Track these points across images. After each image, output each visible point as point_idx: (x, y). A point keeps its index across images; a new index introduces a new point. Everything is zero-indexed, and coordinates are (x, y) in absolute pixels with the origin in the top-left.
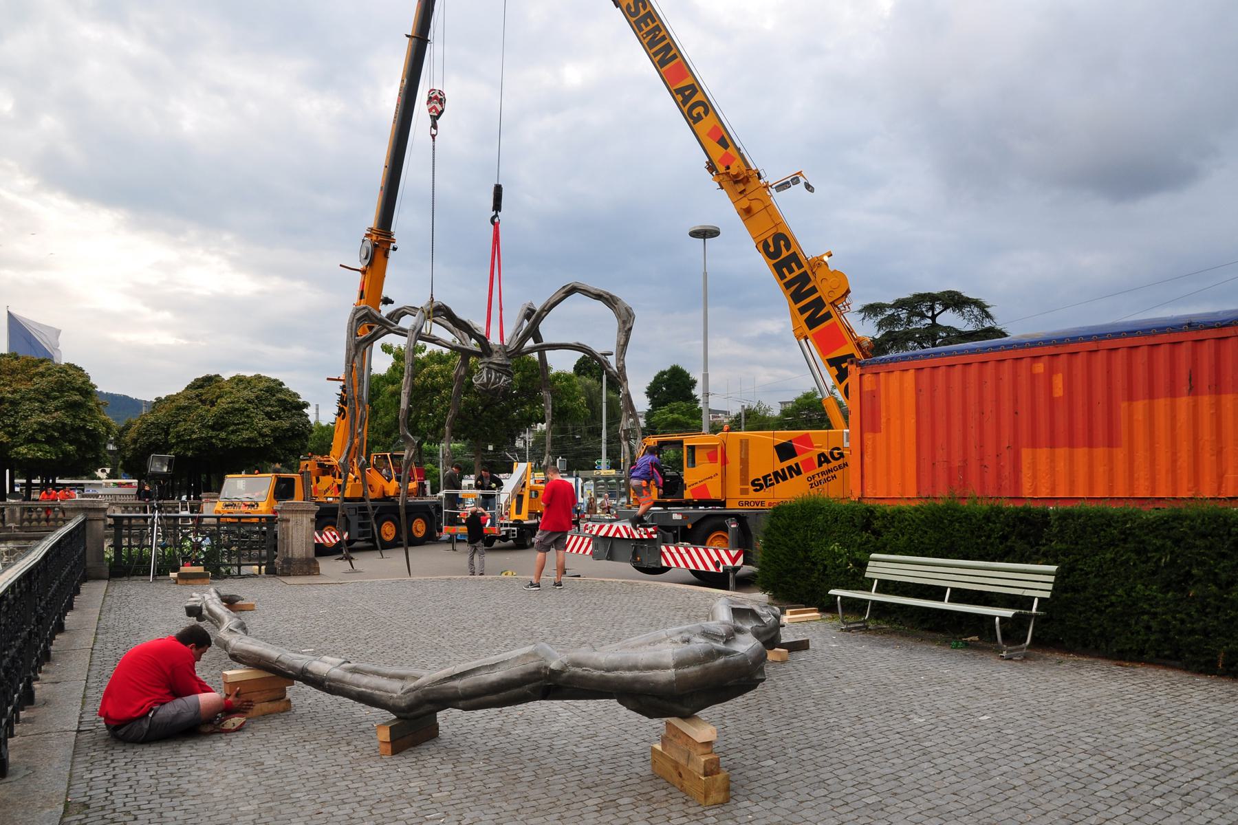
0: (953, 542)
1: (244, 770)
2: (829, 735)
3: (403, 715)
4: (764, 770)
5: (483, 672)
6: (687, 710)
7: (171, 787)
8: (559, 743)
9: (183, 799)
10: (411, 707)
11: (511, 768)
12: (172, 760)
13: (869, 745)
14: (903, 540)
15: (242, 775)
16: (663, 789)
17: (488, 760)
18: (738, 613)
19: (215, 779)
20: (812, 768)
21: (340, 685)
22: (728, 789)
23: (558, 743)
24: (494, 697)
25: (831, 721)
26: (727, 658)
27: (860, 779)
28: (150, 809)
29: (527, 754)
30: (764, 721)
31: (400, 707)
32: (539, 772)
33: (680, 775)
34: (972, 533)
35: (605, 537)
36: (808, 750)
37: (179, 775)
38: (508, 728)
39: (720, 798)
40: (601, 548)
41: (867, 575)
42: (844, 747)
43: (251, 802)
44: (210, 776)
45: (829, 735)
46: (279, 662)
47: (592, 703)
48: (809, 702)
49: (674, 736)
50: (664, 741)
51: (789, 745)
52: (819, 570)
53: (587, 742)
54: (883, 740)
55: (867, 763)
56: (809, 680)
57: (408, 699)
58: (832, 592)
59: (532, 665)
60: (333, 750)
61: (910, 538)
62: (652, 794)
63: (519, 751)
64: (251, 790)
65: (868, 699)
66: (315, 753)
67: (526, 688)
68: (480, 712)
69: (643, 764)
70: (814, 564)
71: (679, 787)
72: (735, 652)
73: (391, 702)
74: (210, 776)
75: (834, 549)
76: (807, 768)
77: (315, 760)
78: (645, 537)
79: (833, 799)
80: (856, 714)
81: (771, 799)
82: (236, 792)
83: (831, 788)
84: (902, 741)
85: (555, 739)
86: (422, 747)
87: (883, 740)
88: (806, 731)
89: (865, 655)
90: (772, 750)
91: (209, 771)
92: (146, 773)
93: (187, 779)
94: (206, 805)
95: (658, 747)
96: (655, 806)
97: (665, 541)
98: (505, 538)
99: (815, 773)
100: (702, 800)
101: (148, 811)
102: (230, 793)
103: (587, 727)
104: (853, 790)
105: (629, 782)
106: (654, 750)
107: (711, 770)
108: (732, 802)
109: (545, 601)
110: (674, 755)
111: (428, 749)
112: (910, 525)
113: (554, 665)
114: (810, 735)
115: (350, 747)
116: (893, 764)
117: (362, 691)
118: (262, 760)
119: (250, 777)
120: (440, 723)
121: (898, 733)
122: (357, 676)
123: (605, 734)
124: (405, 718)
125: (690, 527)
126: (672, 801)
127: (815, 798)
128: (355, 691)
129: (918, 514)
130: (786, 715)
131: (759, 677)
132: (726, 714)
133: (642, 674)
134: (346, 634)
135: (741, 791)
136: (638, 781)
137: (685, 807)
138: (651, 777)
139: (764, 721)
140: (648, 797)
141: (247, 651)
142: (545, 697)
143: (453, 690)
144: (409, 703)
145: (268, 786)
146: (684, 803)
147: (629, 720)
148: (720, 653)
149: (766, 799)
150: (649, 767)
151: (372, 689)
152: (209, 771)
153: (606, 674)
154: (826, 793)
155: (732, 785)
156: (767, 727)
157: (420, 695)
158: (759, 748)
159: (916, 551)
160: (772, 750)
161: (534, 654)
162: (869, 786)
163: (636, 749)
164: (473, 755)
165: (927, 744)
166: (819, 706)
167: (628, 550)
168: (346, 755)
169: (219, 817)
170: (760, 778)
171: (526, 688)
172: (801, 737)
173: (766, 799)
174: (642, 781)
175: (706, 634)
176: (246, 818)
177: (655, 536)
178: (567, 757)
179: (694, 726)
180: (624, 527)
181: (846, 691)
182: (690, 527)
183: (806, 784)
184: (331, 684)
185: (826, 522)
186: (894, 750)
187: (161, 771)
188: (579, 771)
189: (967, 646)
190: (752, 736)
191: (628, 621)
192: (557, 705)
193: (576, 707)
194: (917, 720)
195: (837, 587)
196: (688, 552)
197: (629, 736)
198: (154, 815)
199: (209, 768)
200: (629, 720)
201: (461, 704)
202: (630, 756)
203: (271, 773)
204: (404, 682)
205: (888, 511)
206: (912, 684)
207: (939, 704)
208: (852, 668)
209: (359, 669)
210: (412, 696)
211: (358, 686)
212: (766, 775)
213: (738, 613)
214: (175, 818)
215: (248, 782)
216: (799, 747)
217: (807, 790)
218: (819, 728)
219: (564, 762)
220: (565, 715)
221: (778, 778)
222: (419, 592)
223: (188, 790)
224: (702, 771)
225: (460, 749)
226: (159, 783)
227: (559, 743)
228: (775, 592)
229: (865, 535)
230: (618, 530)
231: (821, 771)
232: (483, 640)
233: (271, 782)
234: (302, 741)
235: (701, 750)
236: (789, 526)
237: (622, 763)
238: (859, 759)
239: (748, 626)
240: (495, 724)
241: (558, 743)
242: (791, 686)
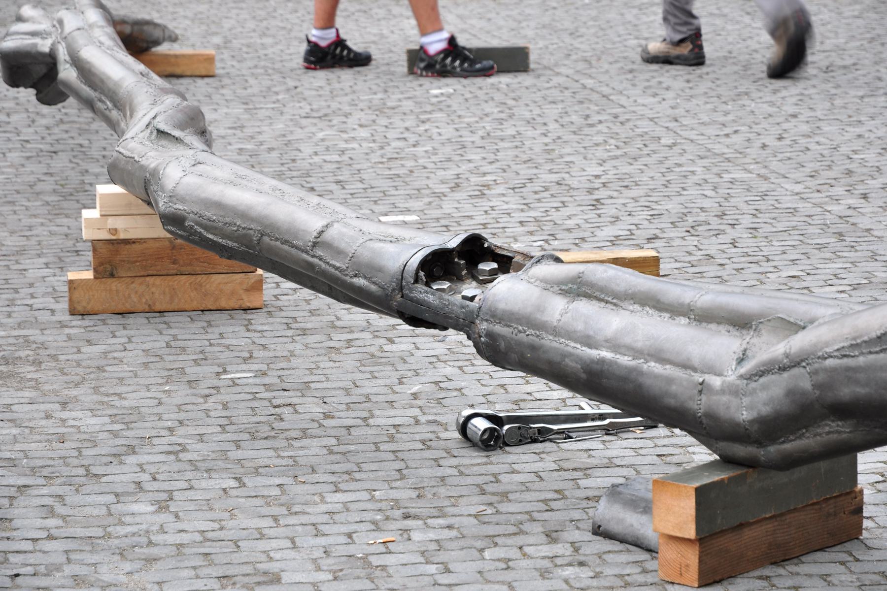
3: (740, 450)
21: (527, 336)
31: (738, 425)
46: (328, 246)
57: (763, 396)
60: (499, 553)
66: (443, 556)
73: (700, 405)
77: (445, 579)
86: (803, 569)
111: (824, 577)
115: (558, 549)
117: (602, 361)
118: (274, 567)
120: (868, 495)
122: (584, 307)
128: (579, 359)
134: (526, 172)
141: (219, 205)
144: (766, 410)
151: (637, 353)
157: (806, 384)
168: (544, 574)
184: (498, 329)
199: (107, 577)
209: (592, 285)
211: (589, 341)
234: (397, 513)
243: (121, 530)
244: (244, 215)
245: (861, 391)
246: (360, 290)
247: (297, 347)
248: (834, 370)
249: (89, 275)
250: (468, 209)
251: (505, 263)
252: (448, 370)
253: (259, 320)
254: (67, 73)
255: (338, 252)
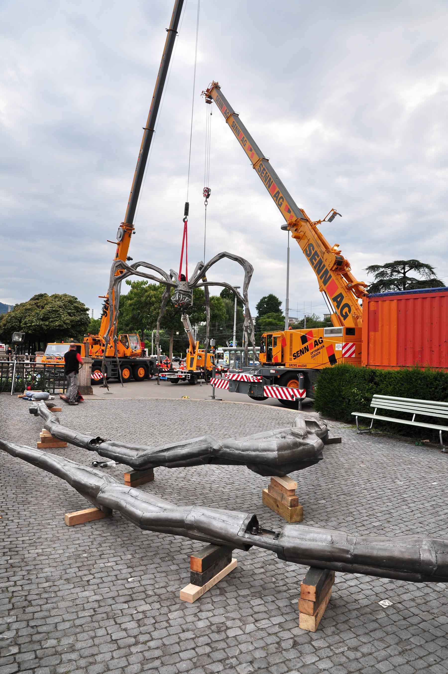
0: (417, 390)
1: (58, 493)
2: (353, 489)
3: (137, 468)
4: (320, 505)
5: (179, 449)
6: (282, 473)
7: (23, 499)
8: (215, 486)
9: (29, 505)
10: (141, 465)
11: (191, 498)
12: (23, 485)
13: (374, 495)
14: (390, 388)
15: (57, 495)
16: (268, 512)
17: (179, 494)
18: (308, 423)
19: (44, 496)
20: (345, 505)
21: (106, 452)
22: (302, 515)
23: (215, 486)
24: (184, 462)
25: (354, 481)
26: (304, 447)
27: (370, 513)
28: (14, 510)
29: (199, 491)
30: (319, 479)
32: (205, 501)
33: (278, 506)
34: (427, 386)
35: (236, 380)
36: (343, 496)
37: (27, 493)
38: (189, 477)
39: (298, 519)
40: (233, 386)
41: (371, 405)
42: (361, 495)
43: (62, 509)
44: (42, 495)
45: (353, 489)
46: (77, 439)
47: (231, 466)
48: (342, 471)
49: (275, 486)
50: (270, 488)
51: (333, 493)
52: (346, 402)
53: (229, 487)
54: (382, 493)
55: (374, 504)
56: (342, 459)
58: (353, 414)
59: (204, 446)
61: (394, 387)
62: (263, 515)
63: (194, 489)
64: (62, 503)
65: (373, 470)
67: (200, 458)
68: (174, 469)
69: (258, 499)
70: (344, 398)
71: (277, 512)
72: (308, 444)
73: (131, 462)
74: (42, 495)
75: (354, 391)
76: (343, 505)
78: (256, 381)
79: (356, 522)
80: (367, 478)
81: (324, 521)
82: (55, 503)
83: (355, 517)
84: (392, 494)
85: (213, 484)
87: (382, 493)
88: (341, 486)
89: (370, 447)
90: (324, 495)
91: (41, 492)
92: (11, 492)
93: (31, 495)
94: (40, 510)
95: (266, 491)
96: (264, 521)
97: (266, 384)
98: (184, 379)
99: (346, 508)
100: (289, 519)
101: (12, 511)
102: (51, 504)
103: (229, 479)
104: (367, 518)
105: (251, 508)
106: (264, 492)
107: (294, 504)
108: (304, 521)
109: (206, 412)
110: (275, 496)
112: (394, 380)
113: (216, 447)
114: (343, 488)
116: (388, 506)
118: (67, 488)
119: (61, 496)
120: (155, 473)
121: (389, 489)
122: (114, 448)
123: (238, 482)
124: (138, 470)
125: (279, 377)
126: (274, 519)
127: (347, 521)
128: (114, 455)
129: (399, 375)
130: (331, 477)
131: (320, 457)
132: (300, 475)
133: (260, 453)
134: (107, 426)
135: (308, 516)
136: (256, 508)
137: (279, 523)
138: (262, 506)
139: (319, 479)
140: (261, 516)
141: (60, 433)
142: (209, 463)
143: (163, 457)
145: (70, 501)
146: (279, 521)
147: (250, 476)
148: (301, 444)
149: (322, 520)
150: (261, 501)
151: (122, 454)
152: (41, 492)
153: (242, 453)
154: (353, 519)
155: (304, 512)
156: (321, 483)
158: (317, 494)
159: (397, 394)
160: (324, 495)
161: (205, 441)
162: (375, 517)
163: (254, 491)
164: (171, 490)
165: (405, 496)
166: (348, 473)
167: (248, 387)
169: (47, 516)
170: (318, 509)
171: (200, 458)
172: (339, 489)
173: (322, 520)
174: (258, 508)
175: (293, 434)
176: (60, 517)
177: (261, 381)
178: (220, 494)
179: (286, 481)
180: (246, 376)
181: (361, 465)
182: (279, 377)
183: (342, 514)
185: (350, 377)
186: (387, 498)
187: (18, 491)
188: (225, 501)
189: (424, 445)
190: (313, 487)
191: (248, 424)
192: (213, 467)
193: (223, 468)
194: (399, 483)
195: (355, 411)
196: (278, 390)
197: (251, 485)
198: (16, 513)
200: (250, 476)
201: (167, 464)
202: (251, 495)
203: (71, 495)
204: (138, 452)
205: (383, 373)
206: (396, 464)
207: (410, 475)
208: (364, 453)
210: (142, 459)
211: (115, 453)
212: (321, 508)
213: (308, 423)
214: (25, 515)
215: (60, 498)
216: (338, 494)
217: (343, 517)
218: (348, 484)
219: (218, 496)
220: (217, 472)
221: (328, 510)
222: (142, 406)
223: (31, 501)
224: (289, 505)
225: (165, 487)
226: (17, 497)
227: (215, 486)
228: (323, 412)
229: (371, 385)
230: (242, 377)
231: (350, 507)
232: (175, 431)
233: (72, 499)
235: (289, 493)
236: (331, 378)
237: (247, 498)
238: (369, 502)
239: (313, 430)
240: (182, 475)
241: (215, 486)
242: (332, 462)
243: (44, 483)
244: (64, 434)
245: (154, 459)
246: (81, 445)
247: (72, 453)
248: (150, 456)
249: (40, 442)
250: (98, 431)
251: (103, 441)
252: (94, 456)
253: (66, 449)
254: (39, 412)
255: (78, 440)
